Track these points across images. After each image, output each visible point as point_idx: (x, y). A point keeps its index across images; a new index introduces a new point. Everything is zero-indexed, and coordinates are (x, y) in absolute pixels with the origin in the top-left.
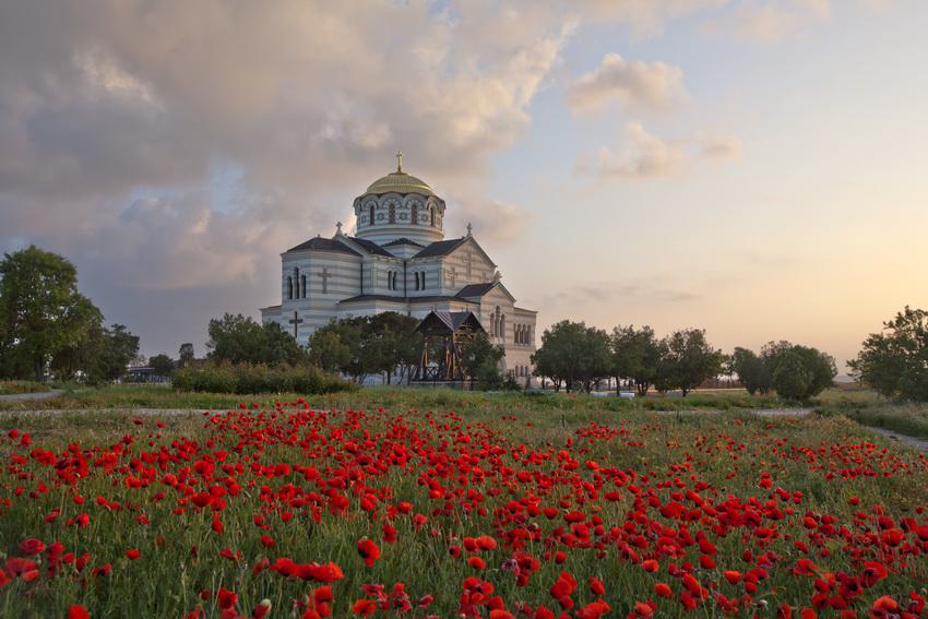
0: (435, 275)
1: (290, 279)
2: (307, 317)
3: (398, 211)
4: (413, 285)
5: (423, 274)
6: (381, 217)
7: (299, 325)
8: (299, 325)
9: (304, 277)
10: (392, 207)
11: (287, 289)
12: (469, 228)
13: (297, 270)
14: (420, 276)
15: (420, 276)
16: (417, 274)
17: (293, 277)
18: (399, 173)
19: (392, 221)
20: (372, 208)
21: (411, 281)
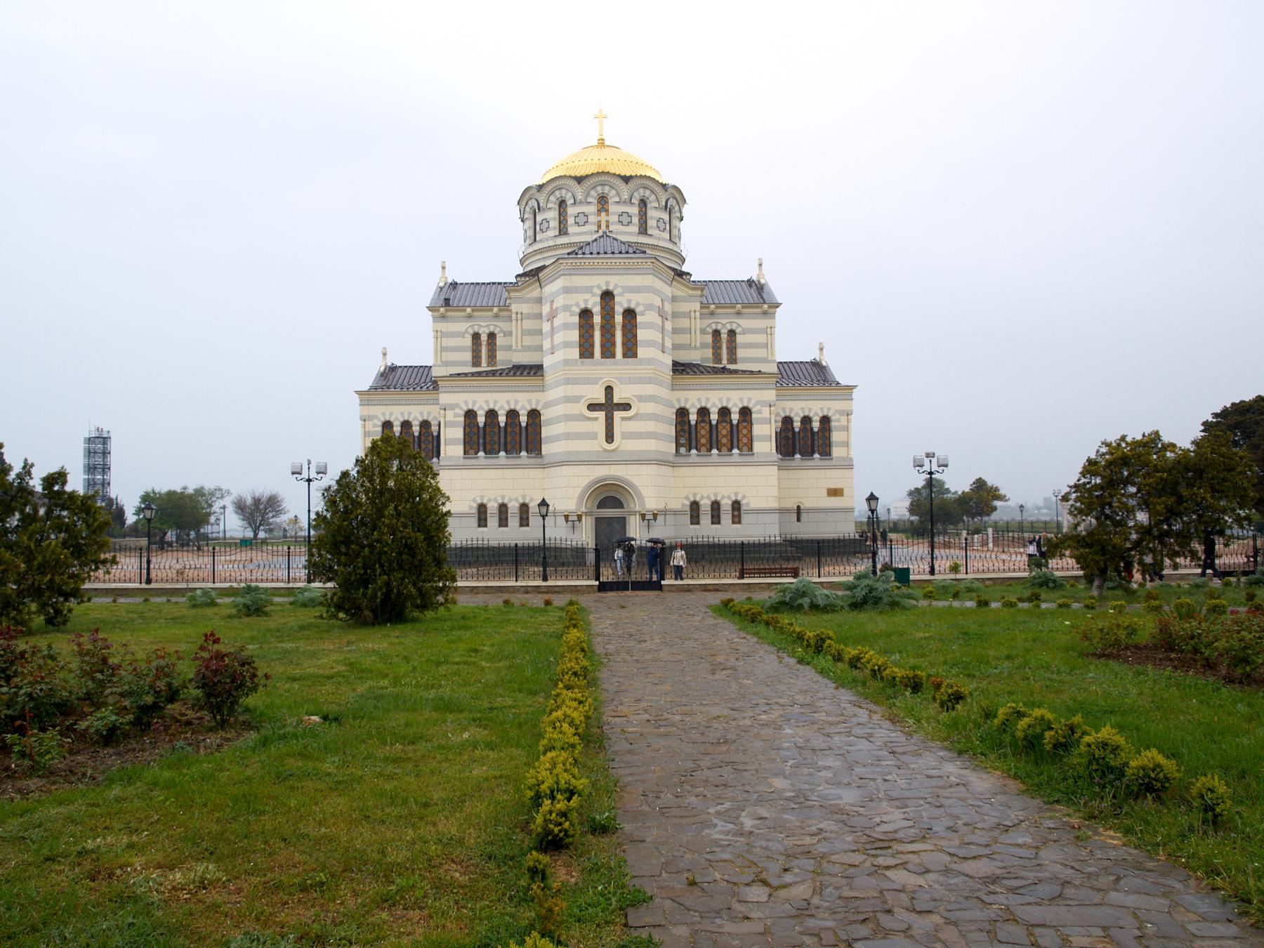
0: (761, 338)
1: (586, 314)
2: (641, 399)
3: (653, 214)
4: (709, 353)
5: (732, 333)
6: (625, 219)
7: (618, 415)
8: (618, 415)
9: (630, 314)
10: (643, 203)
11: (574, 335)
12: (760, 265)
13: (607, 296)
14: (724, 336)
15: (724, 336)
16: (716, 333)
17: (597, 310)
18: (601, 143)
19: (643, 230)
20: (603, 201)
21: (703, 346)
